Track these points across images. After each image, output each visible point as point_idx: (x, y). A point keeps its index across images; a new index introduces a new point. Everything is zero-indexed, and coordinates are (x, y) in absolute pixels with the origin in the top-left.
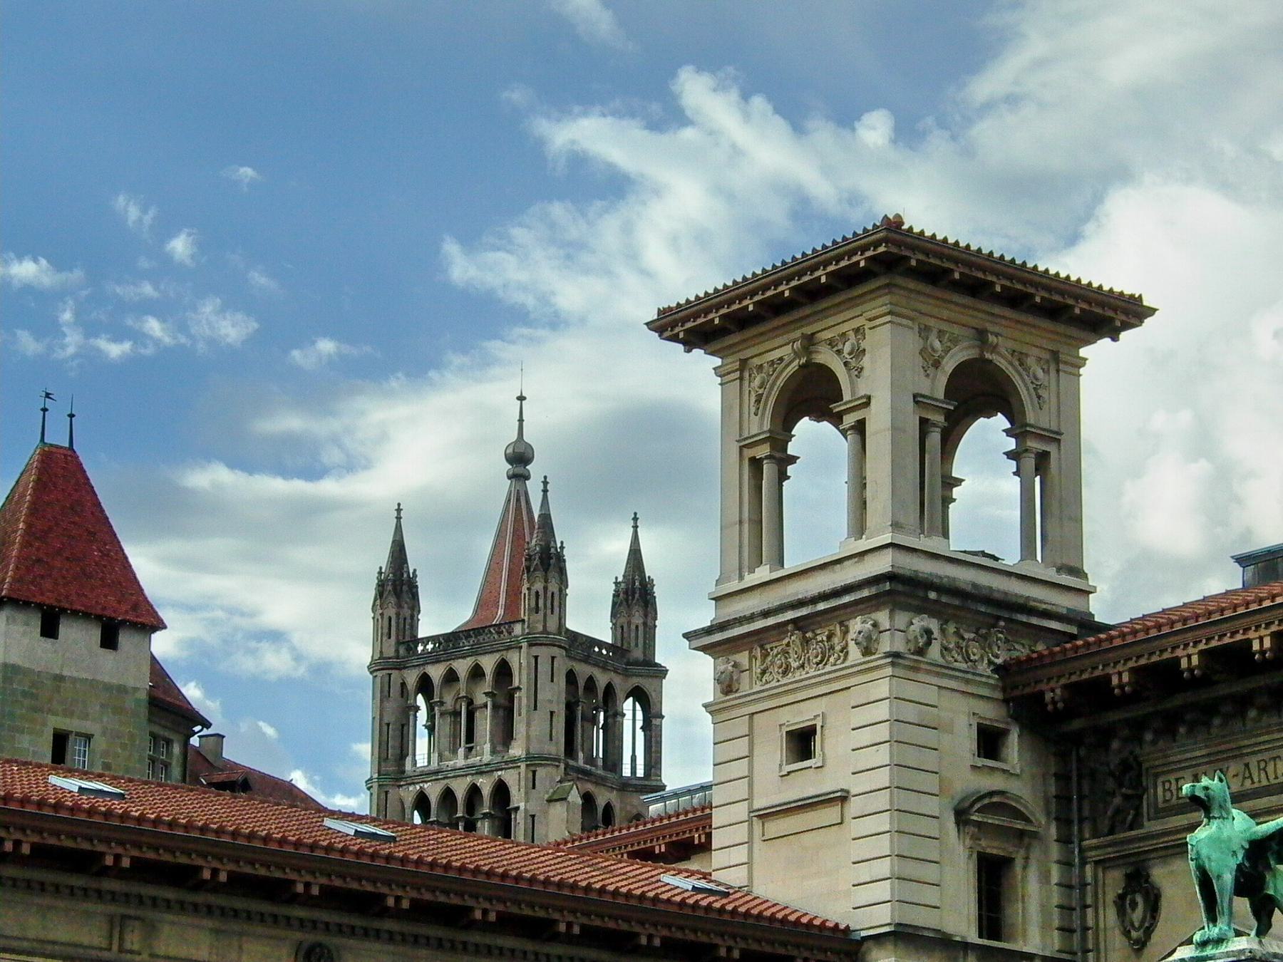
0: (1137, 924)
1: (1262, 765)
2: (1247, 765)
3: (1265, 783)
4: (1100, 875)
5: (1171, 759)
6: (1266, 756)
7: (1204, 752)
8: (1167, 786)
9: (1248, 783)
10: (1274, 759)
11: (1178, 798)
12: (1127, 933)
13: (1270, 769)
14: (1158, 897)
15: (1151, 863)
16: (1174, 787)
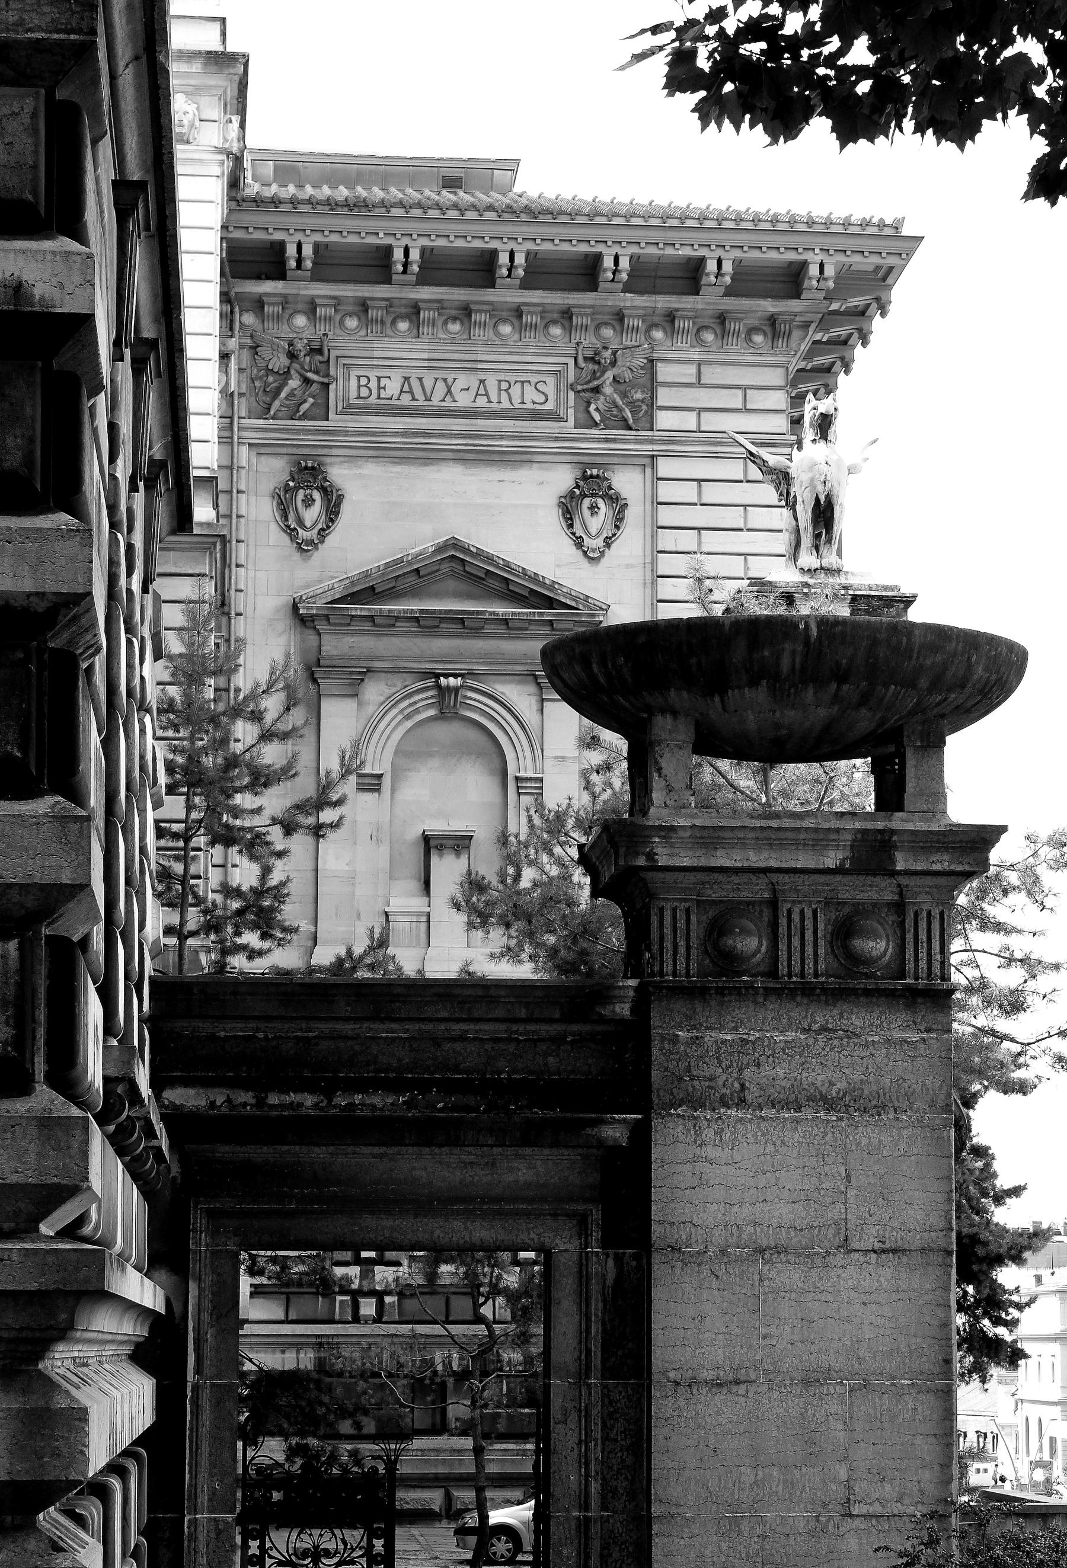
0: (308, 524)
1: (504, 386)
2: (482, 381)
3: (505, 404)
4: (254, 460)
5: (376, 354)
6: (512, 377)
7: (425, 356)
8: (363, 381)
9: (482, 402)
10: (523, 382)
11: (379, 398)
12: (291, 532)
13: (516, 391)
14: (340, 498)
15: (328, 460)
16: (373, 385)
